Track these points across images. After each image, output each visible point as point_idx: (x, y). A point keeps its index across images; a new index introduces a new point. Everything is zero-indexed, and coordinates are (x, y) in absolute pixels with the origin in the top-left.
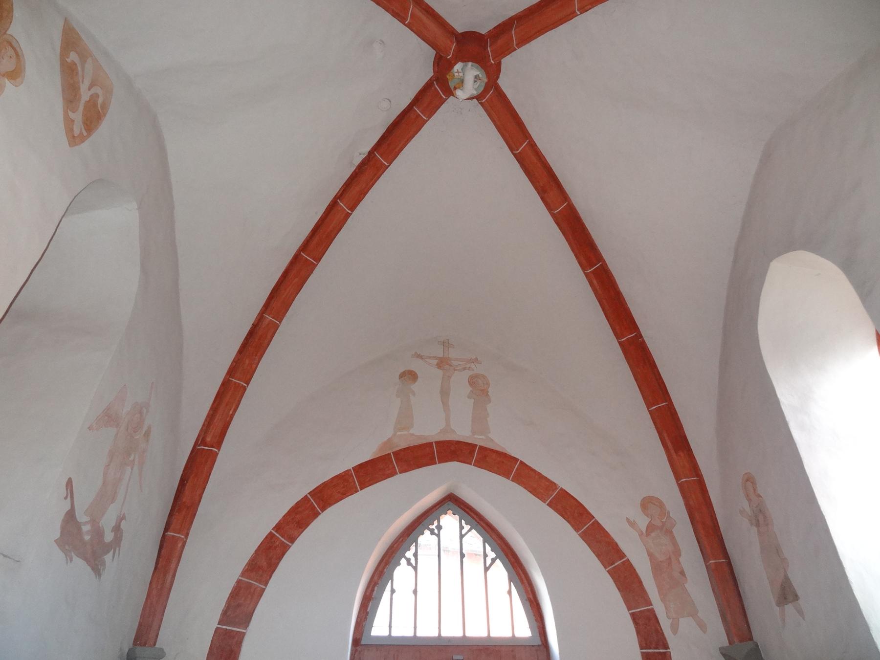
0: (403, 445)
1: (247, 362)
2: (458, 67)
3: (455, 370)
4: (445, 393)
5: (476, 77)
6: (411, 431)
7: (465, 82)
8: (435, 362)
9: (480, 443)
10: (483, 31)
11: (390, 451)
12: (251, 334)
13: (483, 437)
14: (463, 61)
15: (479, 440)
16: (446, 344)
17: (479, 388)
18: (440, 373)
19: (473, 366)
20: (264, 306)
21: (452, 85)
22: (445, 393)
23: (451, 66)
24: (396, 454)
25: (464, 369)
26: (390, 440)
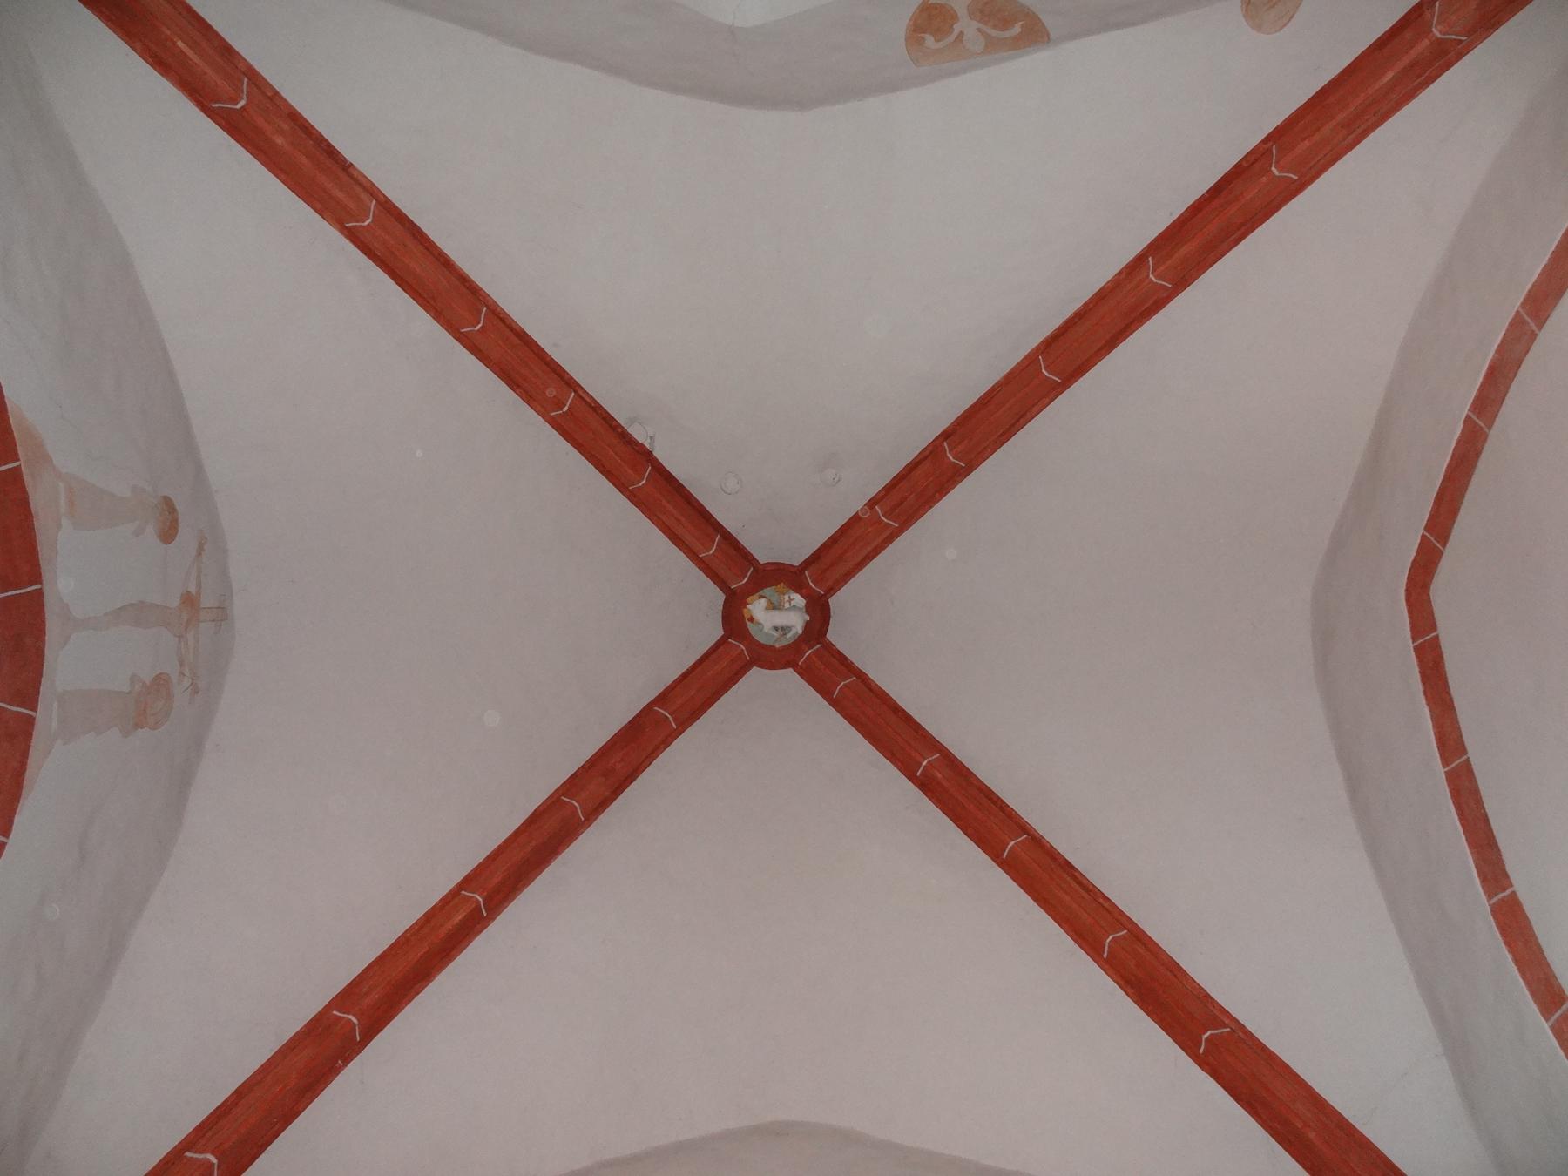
0: (37, 500)
1: (286, 127)
2: (798, 600)
3: (180, 637)
4: (138, 613)
5: (784, 630)
6: (64, 522)
7: (776, 613)
8: (193, 590)
9: (39, 716)
10: (831, 636)
11: (22, 463)
12: (332, 152)
13: (55, 724)
14: (807, 606)
15: (47, 716)
16: (222, 614)
17: (147, 704)
18: (175, 602)
19: (186, 682)
20: (388, 201)
21: (767, 591)
22: (138, 613)
23: (799, 587)
24: (16, 475)
25: (182, 664)
26: (47, 459)
